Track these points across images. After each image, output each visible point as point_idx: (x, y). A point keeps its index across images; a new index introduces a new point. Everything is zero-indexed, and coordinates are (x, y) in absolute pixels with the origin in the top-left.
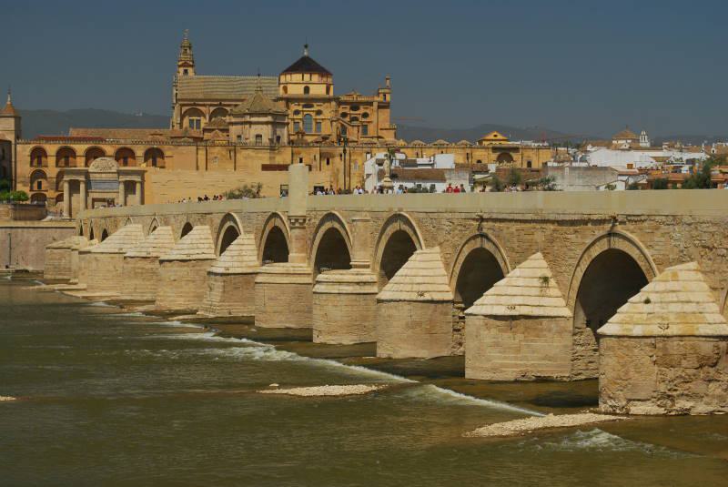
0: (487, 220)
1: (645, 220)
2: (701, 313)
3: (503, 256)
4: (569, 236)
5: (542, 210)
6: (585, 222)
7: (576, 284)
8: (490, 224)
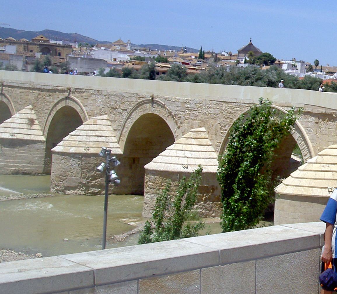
0: (6, 86)
1: (84, 92)
2: (107, 142)
3: (12, 106)
4: (46, 98)
5: (33, 82)
6: (55, 91)
7: (49, 123)
8: (7, 88)
